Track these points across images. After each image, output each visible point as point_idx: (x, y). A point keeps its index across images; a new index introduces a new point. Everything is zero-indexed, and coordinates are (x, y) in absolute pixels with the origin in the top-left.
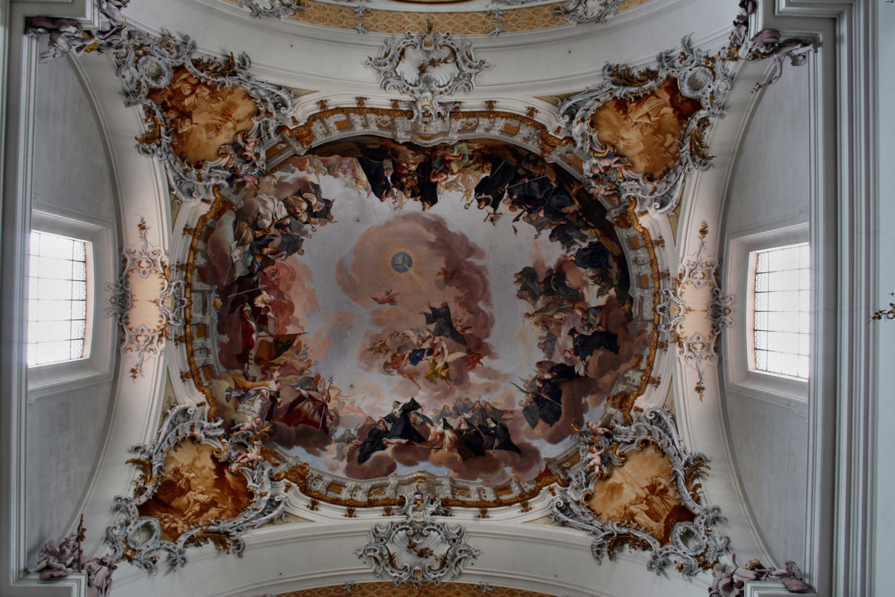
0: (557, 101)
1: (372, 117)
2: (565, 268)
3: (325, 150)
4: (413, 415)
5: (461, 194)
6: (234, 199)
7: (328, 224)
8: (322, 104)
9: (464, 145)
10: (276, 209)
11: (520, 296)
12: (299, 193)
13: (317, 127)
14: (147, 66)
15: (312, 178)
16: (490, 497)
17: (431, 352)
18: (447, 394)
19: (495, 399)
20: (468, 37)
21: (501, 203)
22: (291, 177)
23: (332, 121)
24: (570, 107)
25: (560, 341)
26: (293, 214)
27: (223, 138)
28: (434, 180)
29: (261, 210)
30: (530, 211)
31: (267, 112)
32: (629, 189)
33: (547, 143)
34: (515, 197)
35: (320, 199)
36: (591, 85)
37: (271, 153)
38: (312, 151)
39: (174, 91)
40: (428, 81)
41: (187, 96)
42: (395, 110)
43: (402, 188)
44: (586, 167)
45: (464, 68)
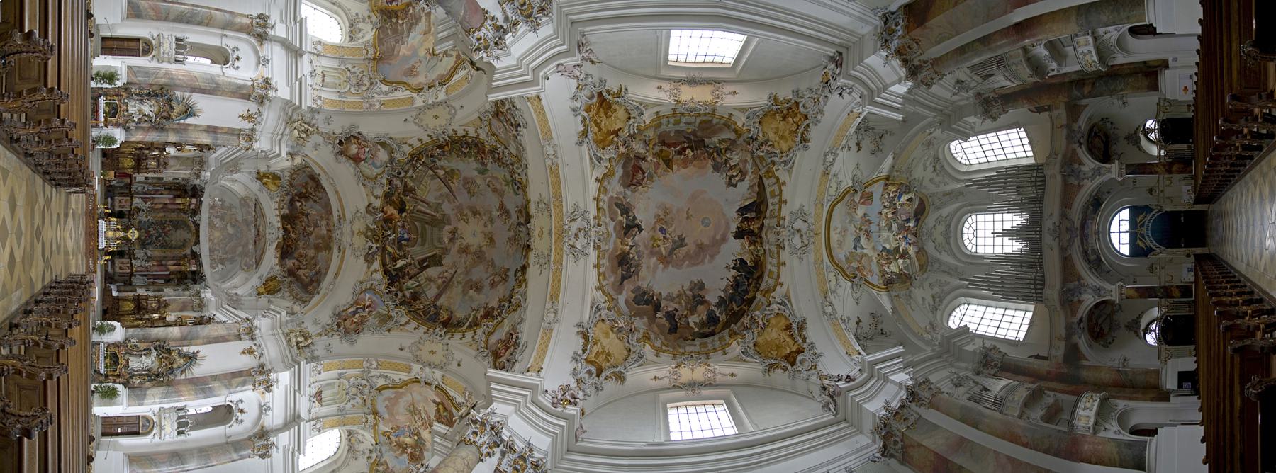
1: (777, 206)
2: (706, 305)
3: (761, 184)
4: (636, 229)
7: (725, 186)
8: (784, 183)
9: (763, 252)
11: (691, 282)
12: (741, 171)
13: (773, 180)
15: (748, 178)
16: (601, 270)
17: (665, 238)
18: (646, 247)
19: (643, 273)
20: (813, 253)
22: (749, 168)
23: (776, 188)
25: (671, 304)
32: (748, 335)
33: (766, 293)
35: (738, 181)
37: (761, 158)
38: (761, 178)
40: (794, 234)
42: (780, 218)
44: (757, 313)
45: (800, 251)
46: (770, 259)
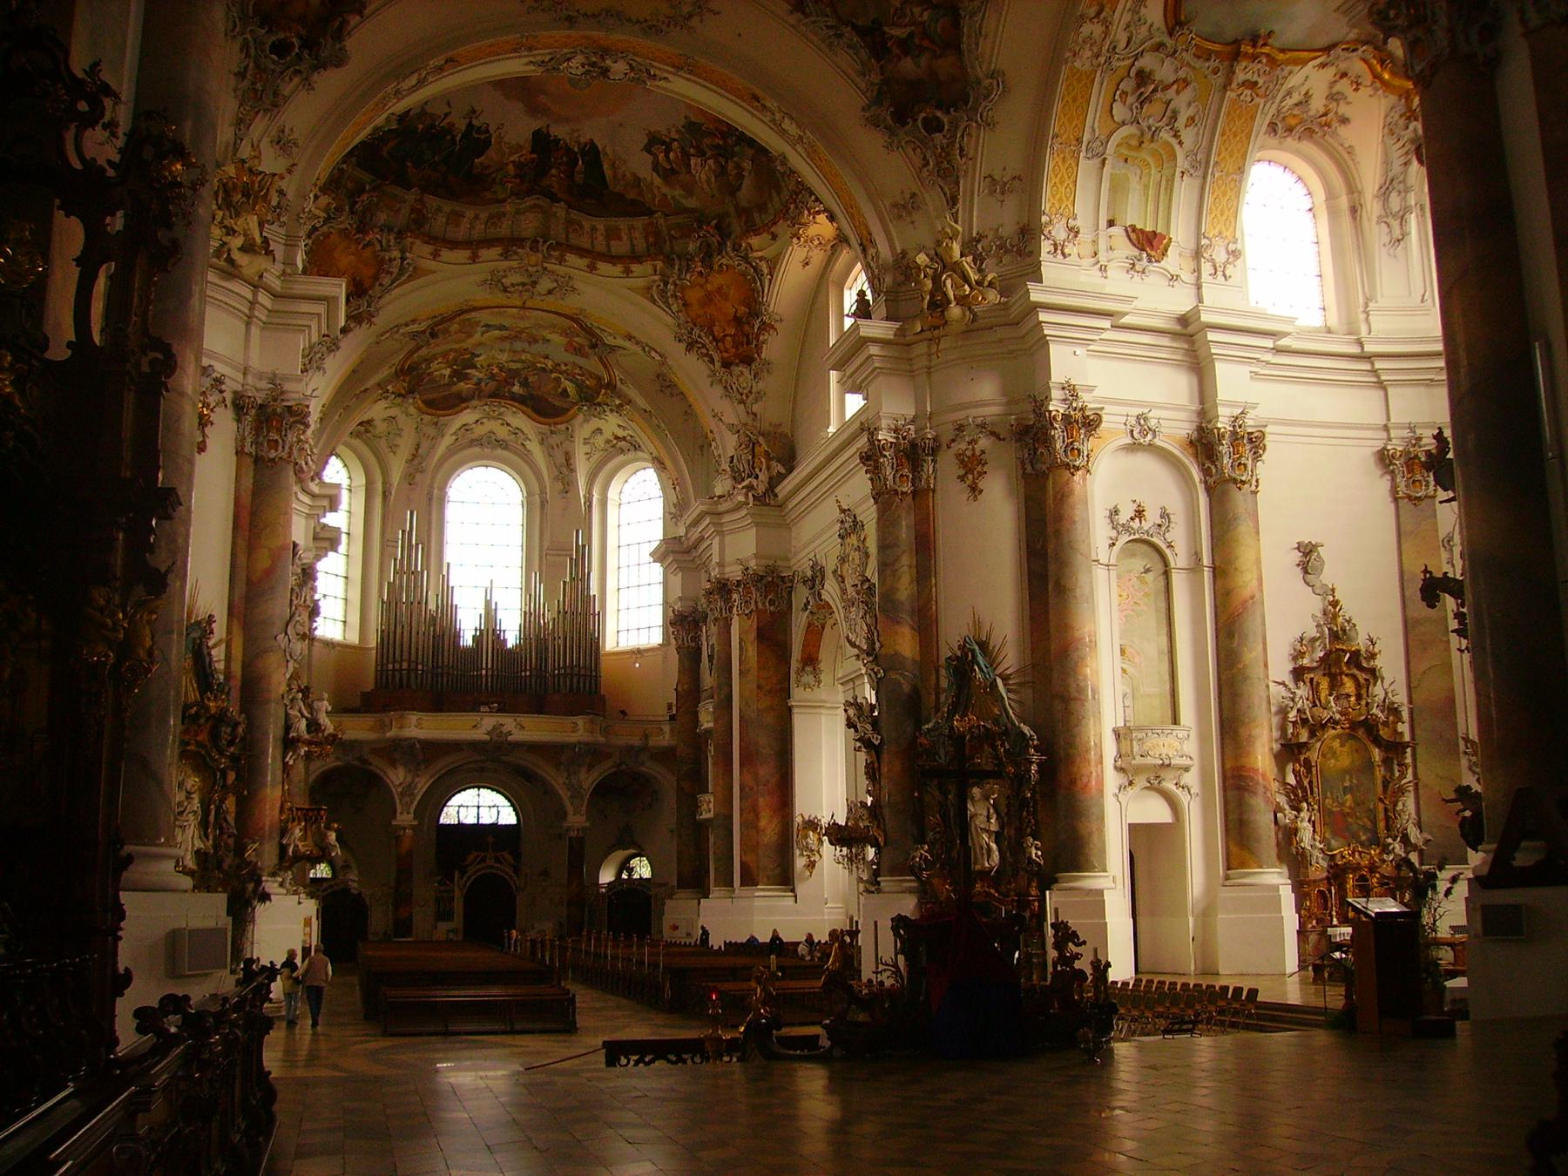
0: (417, 273)
3: (636, 208)
5: (506, 139)
6: (732, 210)
7: (652, 130)
10: (699, 169)
14: (745, 385)
15: (658, 181)
21: (463, 129)
24: (403, 275)
26: (686, 157)
27: (718, 280)
28: (534, 156)
29: (713, 179)
30: (433, 126)
31: (676, 285)
34: (449, 137)
35: (655, 157)
36: (387, 298)
38: (650, 213)
39: (737, 349)
41: (730, 335)
43: (569, 151)
46: (484, 216)
